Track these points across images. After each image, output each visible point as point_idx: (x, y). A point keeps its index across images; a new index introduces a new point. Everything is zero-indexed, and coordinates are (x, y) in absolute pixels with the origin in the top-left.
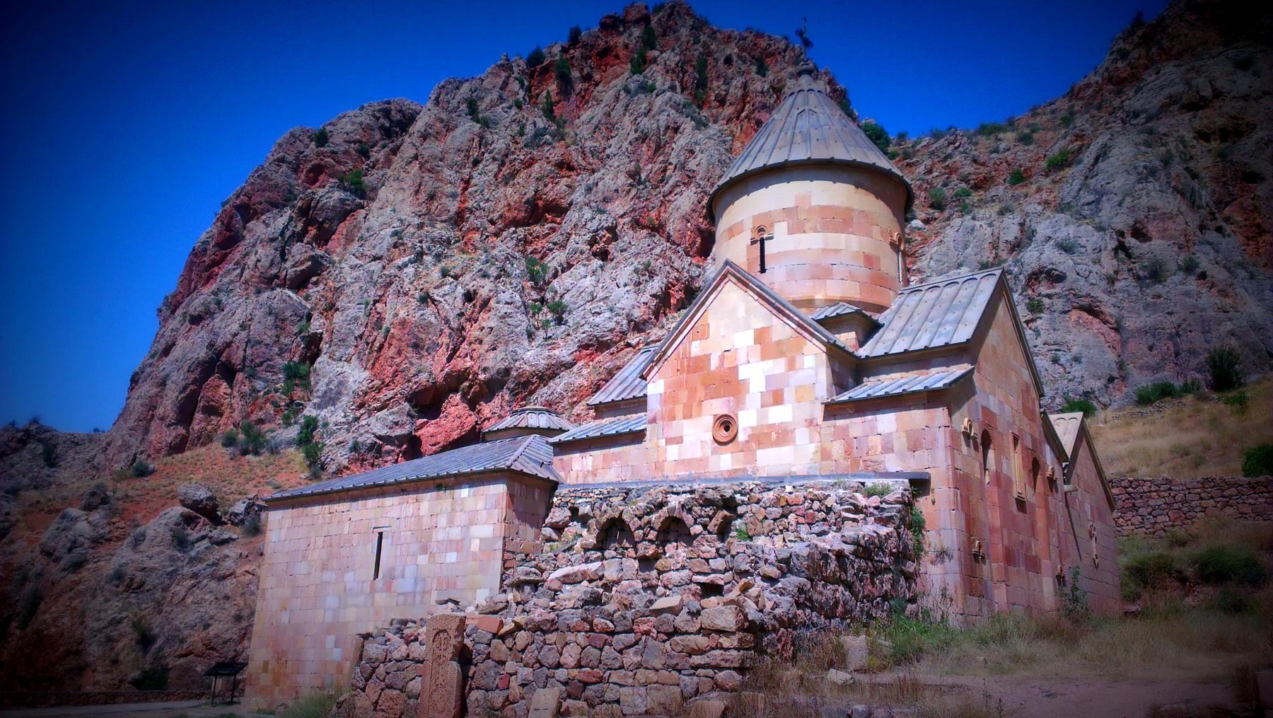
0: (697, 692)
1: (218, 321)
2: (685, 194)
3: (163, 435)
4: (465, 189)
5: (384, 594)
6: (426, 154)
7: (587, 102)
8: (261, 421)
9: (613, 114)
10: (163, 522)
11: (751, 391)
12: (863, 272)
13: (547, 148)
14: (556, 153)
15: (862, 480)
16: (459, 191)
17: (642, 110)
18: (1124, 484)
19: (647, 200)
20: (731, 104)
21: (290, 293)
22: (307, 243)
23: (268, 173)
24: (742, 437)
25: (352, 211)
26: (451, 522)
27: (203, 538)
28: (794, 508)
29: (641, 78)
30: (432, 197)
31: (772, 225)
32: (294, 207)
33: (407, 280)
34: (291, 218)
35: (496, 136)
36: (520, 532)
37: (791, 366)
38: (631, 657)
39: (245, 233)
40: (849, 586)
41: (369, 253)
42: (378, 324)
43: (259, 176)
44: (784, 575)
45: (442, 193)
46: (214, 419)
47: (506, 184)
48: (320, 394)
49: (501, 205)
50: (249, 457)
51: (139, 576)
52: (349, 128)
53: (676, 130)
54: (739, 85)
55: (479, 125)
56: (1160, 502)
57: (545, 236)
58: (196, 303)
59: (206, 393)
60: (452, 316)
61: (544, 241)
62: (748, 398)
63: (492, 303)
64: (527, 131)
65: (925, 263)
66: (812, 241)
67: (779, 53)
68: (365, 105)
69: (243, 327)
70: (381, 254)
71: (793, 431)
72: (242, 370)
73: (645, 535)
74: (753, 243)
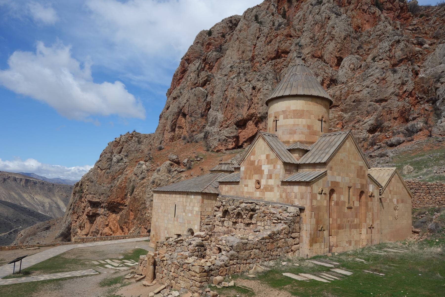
2: (331, 44)
3: (168, 135)
4: (255, 48)
6: (241, 37)
7: (298, 10)
9: (306, 14)
10: (165, 166)
11: (265, 174)
12: (306, 131)
13: (282, 30)
14: (285, 33)
15: (287, 206)
16: (252, 49)
17: (316, 12)
18: (427, 184)
19: (317, 47)
20: (353, 4)
21: (201, 88)
22: (206, 71)
23: (194, 47)
24: (262, 187)
25: (219, 58)
26: (190, 205)
28: (267, 215)
30: (243, 52)
32: (201, 59)
33: (234, 83)
34: (200, 63)
35: (265, 27)
36: (206, 210)
37: (274, 167)
38: (182, 274)
40: (259, 249)
41: (223, 74)
44: (231, 250)
45: (247, 50)
47: (268, 45)
48: (210, 122)
52: (219, 28)
53: (329, 18)
56: (438, 192)
57: (281, 63)
59: (178, 122)
60: (248, 95)
62: (264, 175)
64: (275, 24)
65: (427, 63)
66: (290, 121)
69: (187, 101)
70: (227, 74)
71: (274, 188)
73: (233, 216)
74: (274, 121)
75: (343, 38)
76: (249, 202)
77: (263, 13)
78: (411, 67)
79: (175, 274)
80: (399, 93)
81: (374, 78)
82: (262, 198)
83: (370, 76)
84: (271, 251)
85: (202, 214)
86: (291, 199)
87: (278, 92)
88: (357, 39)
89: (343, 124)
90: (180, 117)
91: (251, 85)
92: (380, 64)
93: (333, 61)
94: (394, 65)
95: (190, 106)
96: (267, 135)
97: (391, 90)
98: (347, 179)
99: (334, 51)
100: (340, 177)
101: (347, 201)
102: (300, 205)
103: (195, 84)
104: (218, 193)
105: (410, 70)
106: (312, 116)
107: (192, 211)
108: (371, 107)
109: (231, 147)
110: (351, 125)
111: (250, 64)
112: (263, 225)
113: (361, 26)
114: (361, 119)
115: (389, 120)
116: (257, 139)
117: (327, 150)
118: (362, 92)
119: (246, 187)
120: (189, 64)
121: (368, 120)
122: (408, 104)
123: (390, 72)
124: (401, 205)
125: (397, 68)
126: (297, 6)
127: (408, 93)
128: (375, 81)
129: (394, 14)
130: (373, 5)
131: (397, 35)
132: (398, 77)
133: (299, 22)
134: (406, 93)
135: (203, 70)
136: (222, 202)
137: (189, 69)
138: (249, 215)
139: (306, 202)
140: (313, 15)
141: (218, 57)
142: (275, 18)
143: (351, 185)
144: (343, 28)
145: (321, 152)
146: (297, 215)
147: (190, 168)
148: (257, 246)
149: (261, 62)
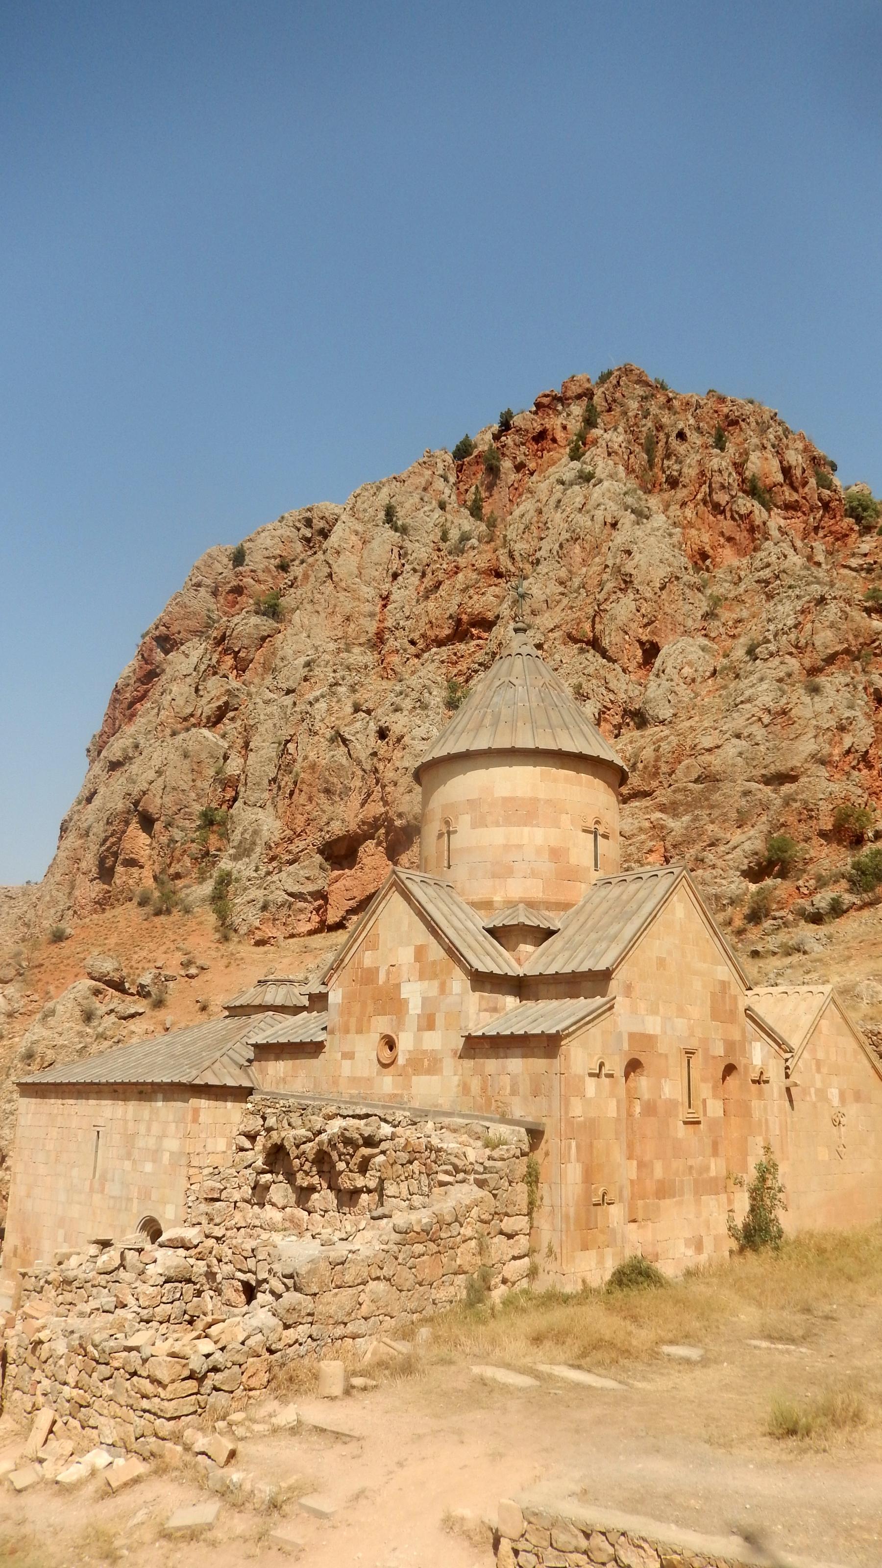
0: (143, 1436)
1: (134, 768)
2: (622, 602)
4: (385, 606)
5: (100, 1195)
7: (520, 495)
8: (178, 876)
10: (72, 996)
11: (411, 1012)
12: (546, 866)
15: (487, 1124)
16: (378, 609)
20: (684, 486)
21: (205, 732)
22: (225, 676)
24: (401, 1061)
25: (269, 636)
26: (149, 1130)
27: (112, 1011)
28: (417, 1155)
29: (575, 464)
31: (457, 818)
34: (207, 649)
35: (417, 544)
37: (443, 989)
38: (107, 1390)
39: (165, 666)
42: (288, 768)
43: (177, 604)
46: (134, 870)
47: (427, 598)
48: (235, 844)
49: (422, 623)
50: (162, 918)
51: (50, 1055)
52: (269, 542)
53: (614, 525)
54: (694, 463)
55: (398, 534)
58: (115, 749)
59: (126, 845)
61: (470, 660)
63: (406, 739)
64: (450, 536)
67: (743, 420)
68: (286, 515)
69: (159, 773)
70: (294, 687)
71: (441, 1060)
72: (158, 819)
73: (302, 1165)
74: (441, 835)
75: (658, 585)
76: (358, 1112)
77: (411, 501)
78: (862, 678)
79: (81, 1392)
80: (831, 755)
81: (756, 709)
82: (402, 1096)
83: (742, 702)
84: (431, 1285)
85: (192, 1164)
86: (498, 1098)
87: (452, 738)
88: (699, 590)
89: (666, 850)
90: (131, 827)
91: (372, 724)
92: (773, 668)
93: (631, 654)
94: (813, 671)
95: (168, 789)
96: (418, 879)
97: (807, 746)
98: (680, 1024)
99: (631, 624)
100: (659, 1019)
101: (682, 1098)
102: (529, 1119)
103: (185, 719)
104: (250, 1085)
105: (860, 687)
106: (564, 817)
107: (156, 1151)
108: (748, 798)
109: (305, 927)
110: (692, 852)
111: (370, 658)
112: (405, 1194)
113: (711, 553)
114: (721, 834)
115: (807, 840)
116: (383, 898)
117: (613, 930)
118: (720, 751)
119: (349, 1062)
120: (167, 653)
121: (743, 838)
122: (859, 791)
123: (802, 691)
124: (853, 1110)
125: (821, 679)
126: (516, 485)
127: (857, 755)
128: (760, 719)
129: (806, 522)
130: (744, 492)
131: (818, 583)
132: (827, 708)
133: (523, 533)
134: (851, 756)
135: (215, 673)
136: (264, 1118)
137: (167, 670)
138: (357, 1159)
139: (550, 1106)
140: (566, 514)
141: (266, 634)
142: (449, 517)
143: (693, 1044)
144: (658, 557)
145: (593, 936)
146: (518, 1154)
147: (159, 1004)
148: (382, 1269)
149: (405, 650)
